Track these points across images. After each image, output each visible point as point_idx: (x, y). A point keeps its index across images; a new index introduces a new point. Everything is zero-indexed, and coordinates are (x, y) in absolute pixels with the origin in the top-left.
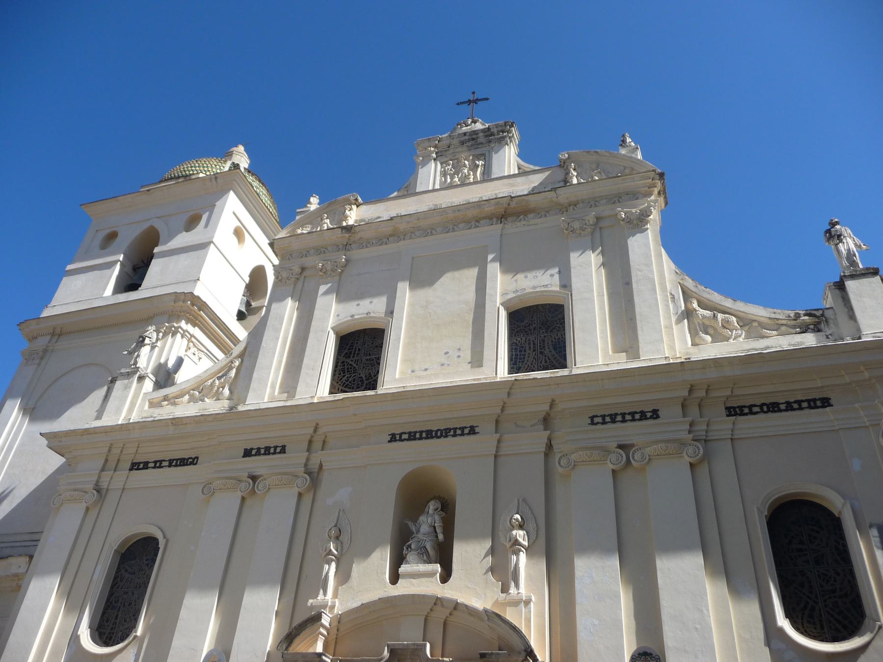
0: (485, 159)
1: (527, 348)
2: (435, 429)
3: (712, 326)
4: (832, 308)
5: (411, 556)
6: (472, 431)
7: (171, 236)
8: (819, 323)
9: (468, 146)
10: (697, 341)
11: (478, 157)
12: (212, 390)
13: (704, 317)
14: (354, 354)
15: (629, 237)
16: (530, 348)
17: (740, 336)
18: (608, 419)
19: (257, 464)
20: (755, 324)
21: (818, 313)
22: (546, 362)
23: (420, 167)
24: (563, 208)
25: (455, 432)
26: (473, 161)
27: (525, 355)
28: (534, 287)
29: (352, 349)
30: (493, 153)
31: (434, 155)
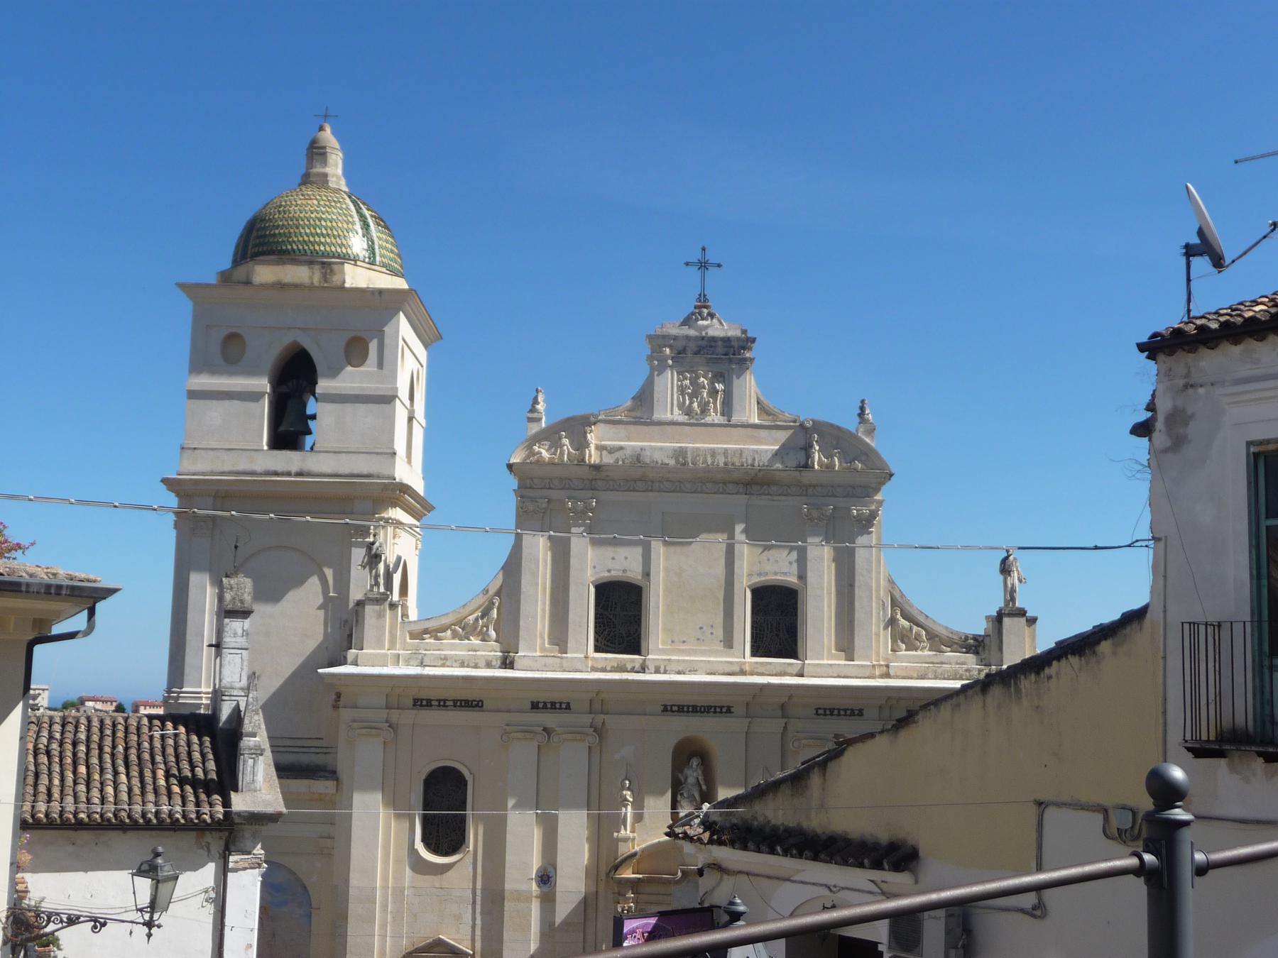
0: (724, 381)
1: (766, 629)
2: (700, 705)
3: (907, 636)
4: (989, 636)
5: (684, 803)
6: (729, 710)
7: (334, 372)
8: (979, 646)
9: (706, 358)
10: (895, 647)
11: (719, 377)
12: (476, 628)
13: (903, 627)
14: (611, 607)
15: (857, 537)
16: (768, 629)
17: (925, 648)
18: (828, 712)
19: (550, 719)
20: (937, 639)
21: (980, 639)
22: (780, 645)
23: (656, 373)
24: (806, 490)
25: (715, 709)
26: (712, 383)
27: (763, 634)
28: (776, 573)
29: (609, 601)
30: (734, 377)
31: (670, 362)
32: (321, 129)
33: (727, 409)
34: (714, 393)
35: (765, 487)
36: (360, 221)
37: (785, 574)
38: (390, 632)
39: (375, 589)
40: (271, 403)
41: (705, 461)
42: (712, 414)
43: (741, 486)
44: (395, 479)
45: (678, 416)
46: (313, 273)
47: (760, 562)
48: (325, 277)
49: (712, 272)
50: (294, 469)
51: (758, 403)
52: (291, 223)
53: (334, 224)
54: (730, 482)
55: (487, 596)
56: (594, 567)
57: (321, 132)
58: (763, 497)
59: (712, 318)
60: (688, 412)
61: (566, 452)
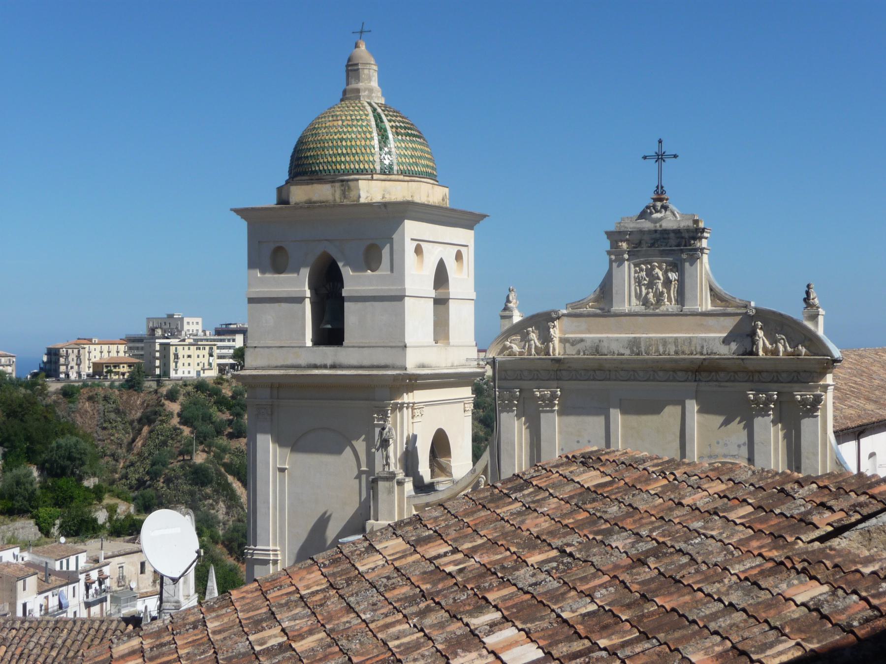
26: (665, 273)
28: (725, 456)
31: (626, 256)
32: (357, 46)
33: (681, 298)
34: (667, 283)
35: (713, 374)
36: (378, 135)
37: (734, 456)
38: (399, 506)
39: (386, 469)
40: (312, 303)
41: (657, 351)
42: (667, 303)
43: (690, 374)
44: (406, 369)
45: (635, 306)
46: (335, 191)
47: (710, 445)
48: (344, 195)
49: (669, 163)
50: (329, 362)
51: (711, 290)
52: (319, 146)
53: (353, 143)
54: (681, 370)
55: (475, 475)
56: (562, 450)
57: (357, 49)
58: (711, 383)
59: (666, 210)
60: (646, 302)
61: (533, 346)
